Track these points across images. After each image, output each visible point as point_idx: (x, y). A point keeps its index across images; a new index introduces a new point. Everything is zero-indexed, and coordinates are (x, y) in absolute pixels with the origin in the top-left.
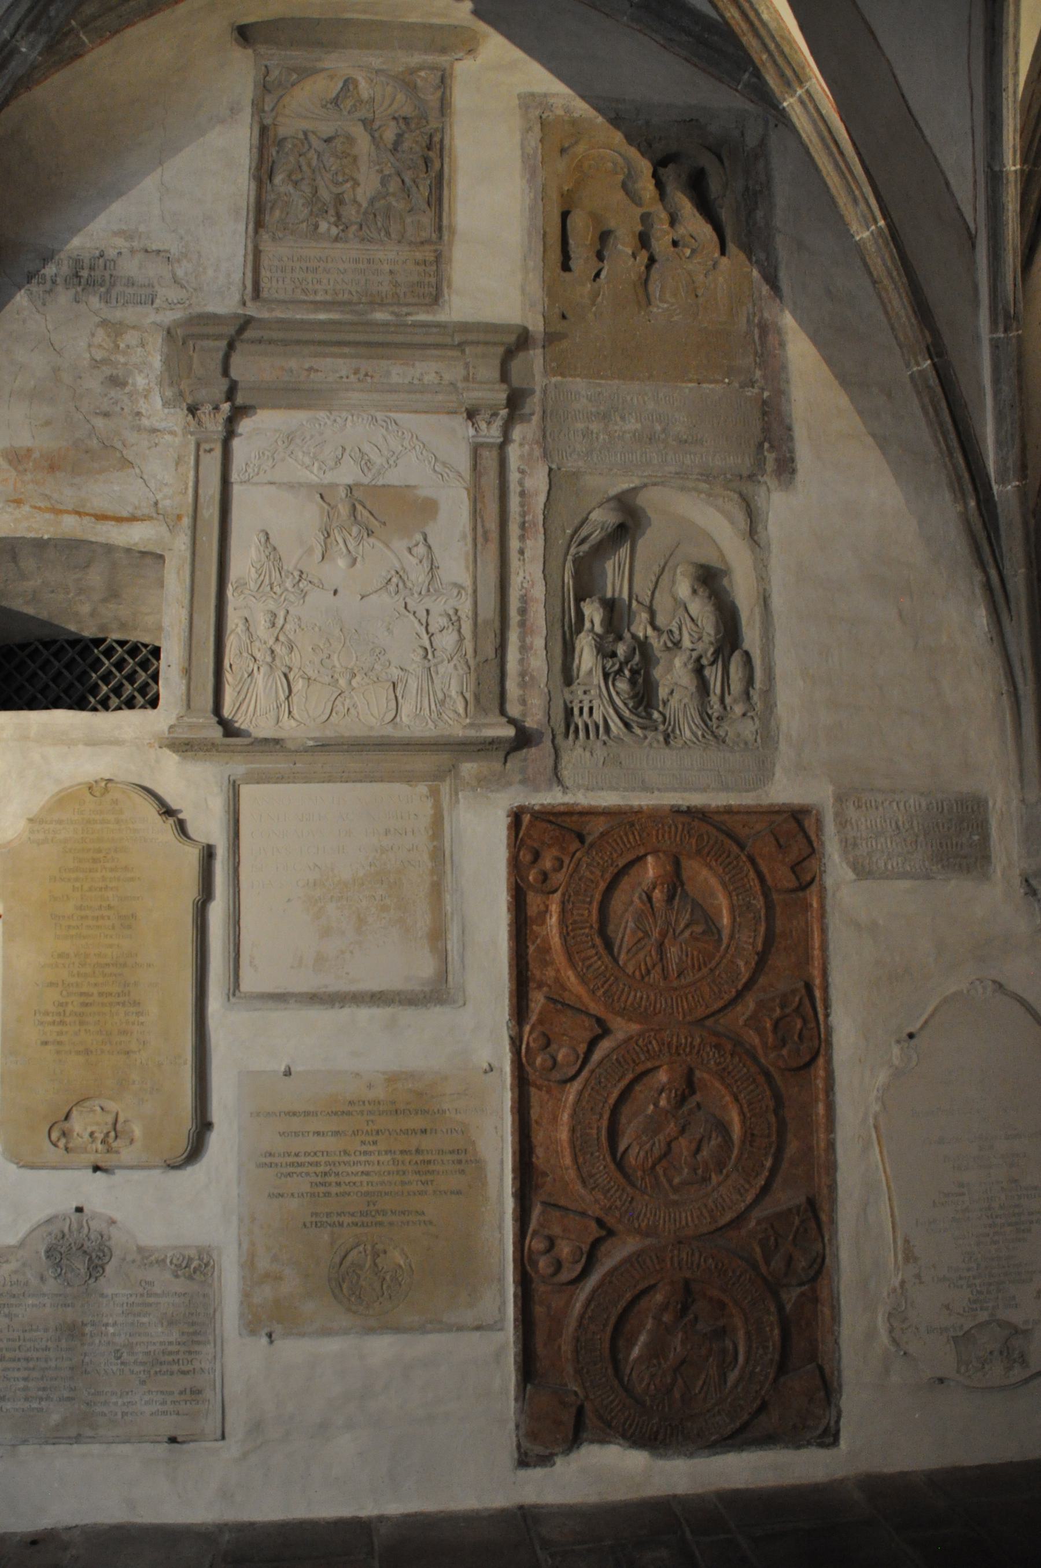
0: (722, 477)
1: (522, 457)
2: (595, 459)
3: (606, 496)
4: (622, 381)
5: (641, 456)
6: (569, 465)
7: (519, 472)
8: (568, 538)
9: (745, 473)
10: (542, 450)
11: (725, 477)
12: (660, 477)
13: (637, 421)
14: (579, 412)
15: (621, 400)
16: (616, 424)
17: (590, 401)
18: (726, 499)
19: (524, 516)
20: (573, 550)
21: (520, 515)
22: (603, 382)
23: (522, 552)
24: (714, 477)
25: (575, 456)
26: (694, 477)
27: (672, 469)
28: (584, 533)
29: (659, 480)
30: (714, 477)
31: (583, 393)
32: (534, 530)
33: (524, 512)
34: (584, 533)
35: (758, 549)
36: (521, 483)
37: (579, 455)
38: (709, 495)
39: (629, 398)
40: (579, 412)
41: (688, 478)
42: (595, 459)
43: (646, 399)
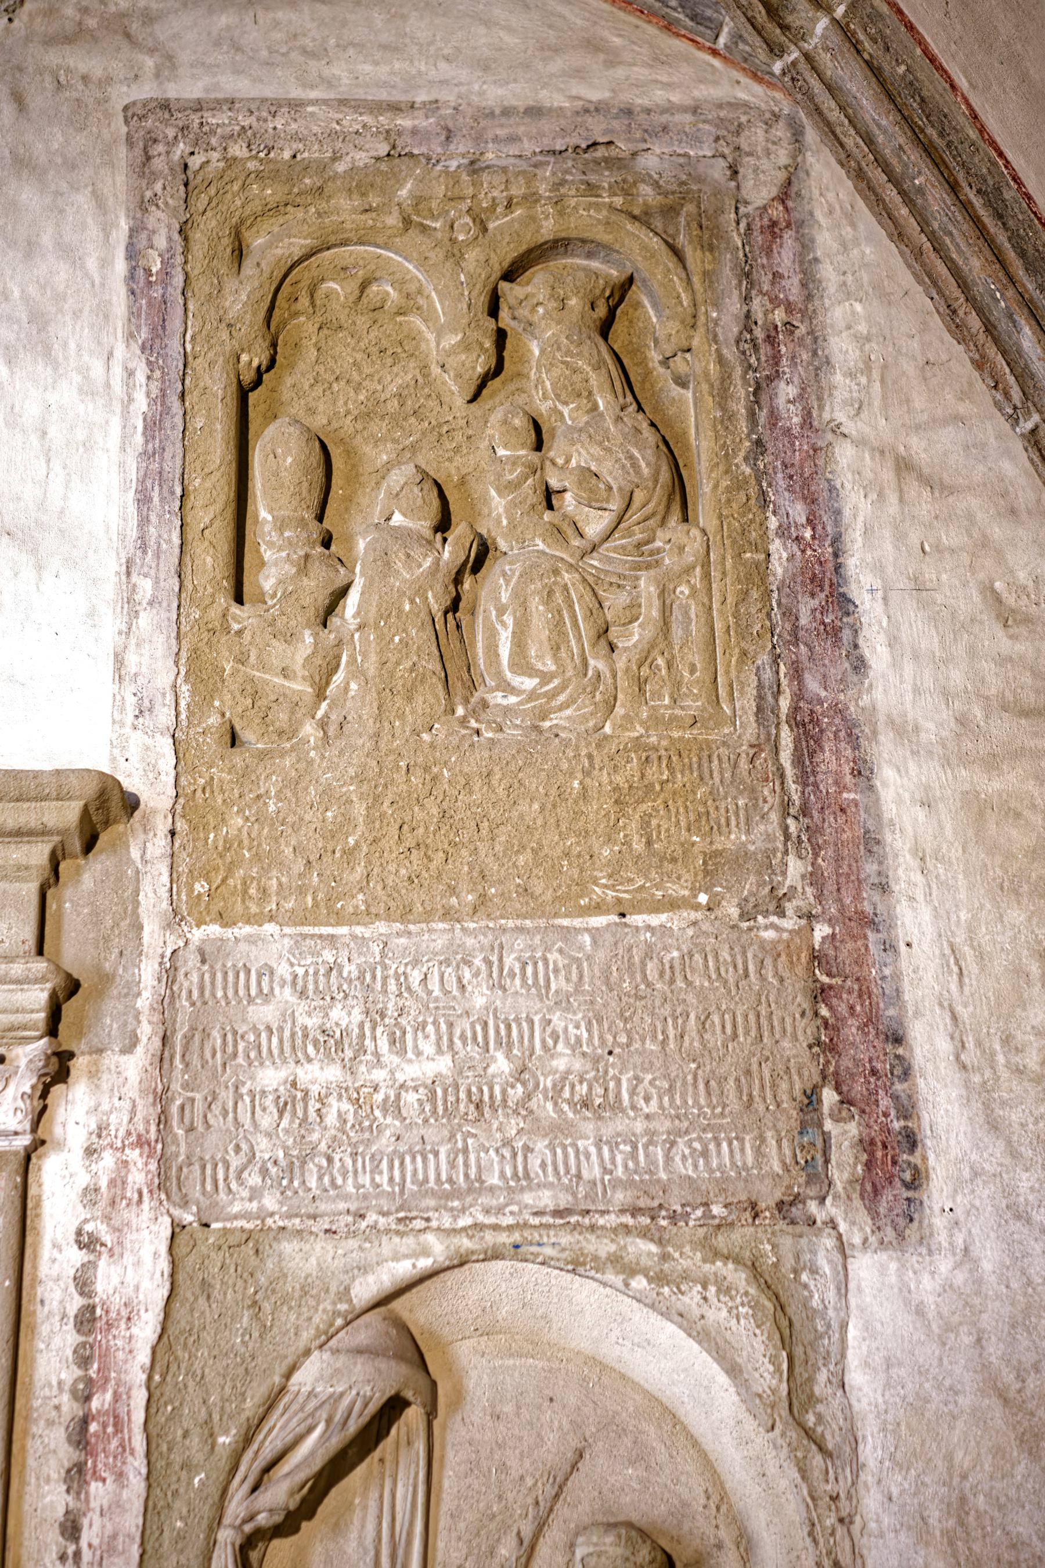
0: (699, 1213)
1: (90, 1195)
2: (313, 1182)
3: (343, 1307)
4: (398, 926)
5: (452, 1165)
6: (236, 1208)
7: (81, 1245)
8: (223, 1461)
9: (769, 1196)
10: (153, 1166)
11: (708, 1215)
12: (510, 1228)
13: (440, 1051)
14: (269, 1030)
15: (392, 987)
16: (379, 1063)
17: (303, 994)
18: (712, 1289)
19: (88, 1399)
20: (236, 1507)
21: (74, 1392)
22: (343, 930)
23: (71, 1528)
24: (673, 1217)
25: (254, 1179)
26: (611, 1220)
27: (546, 1199)
28: (269, 1444)
29: (504, 1238)
30: (673, 1217)
31: (283, 970)
32: (114, 1443)
33: (89, 1382)
34: (269, 1444)
35: (818, 1460)
36: (83, 1283)
37: (264, 1172)
38: (659, 1279)
39: (415, 976)
40: (269, 1030)
41: (593, 1228)
42: (313, 1182)
43: (467, 974)
